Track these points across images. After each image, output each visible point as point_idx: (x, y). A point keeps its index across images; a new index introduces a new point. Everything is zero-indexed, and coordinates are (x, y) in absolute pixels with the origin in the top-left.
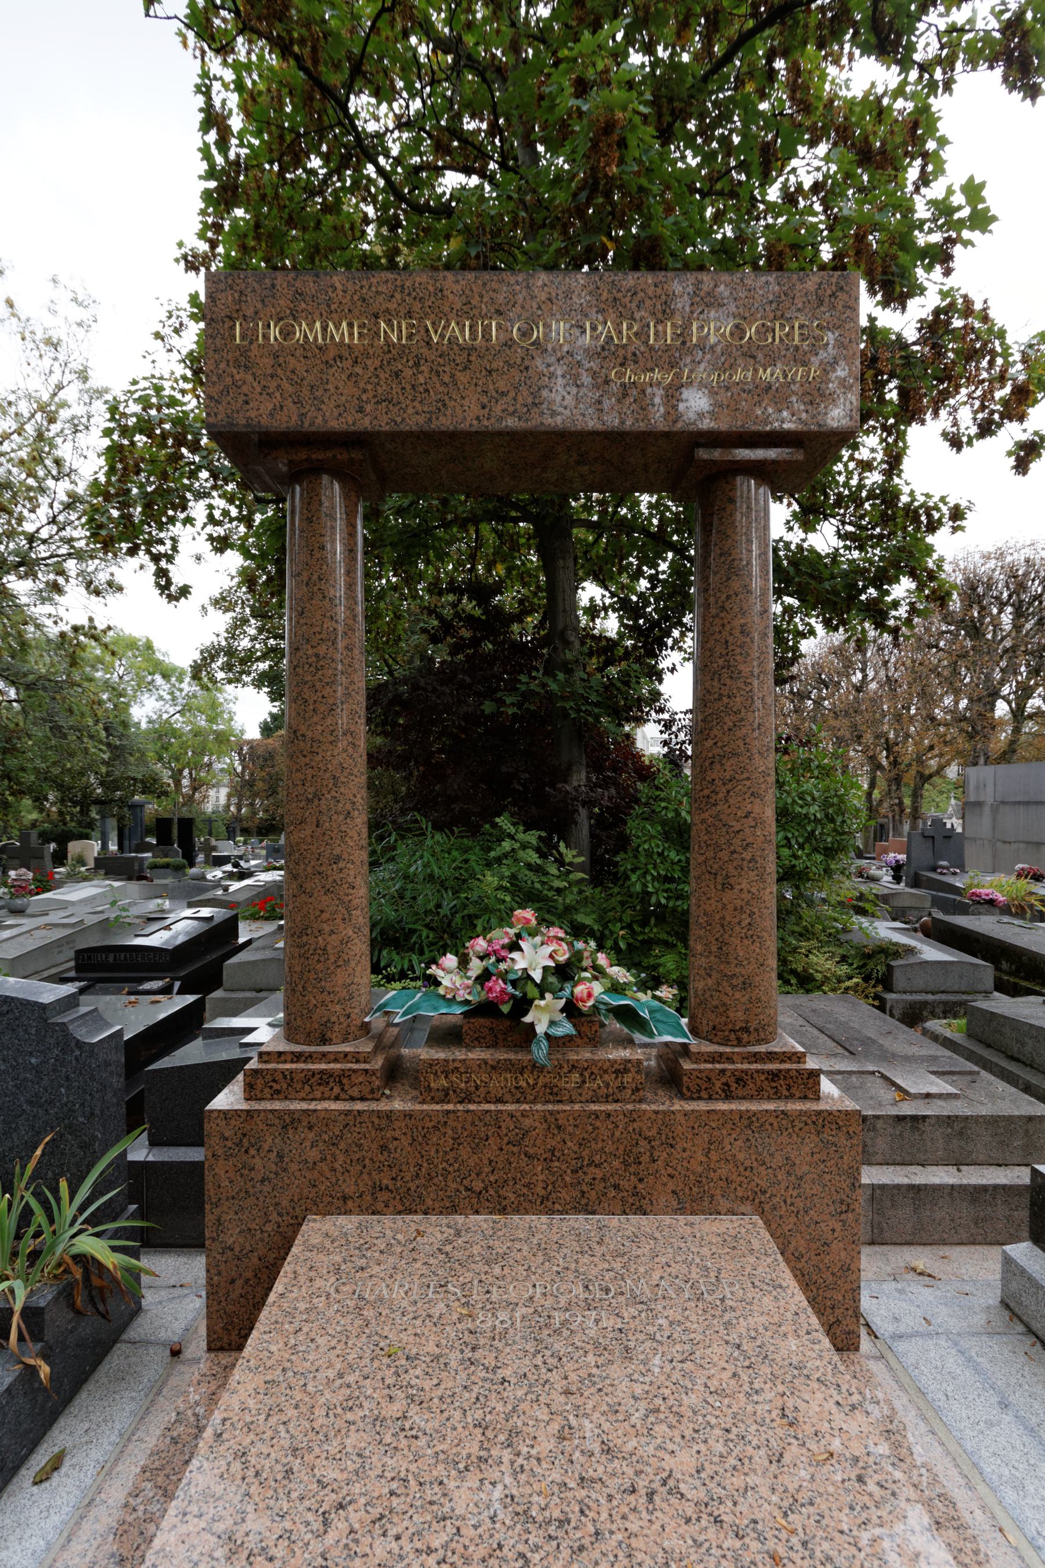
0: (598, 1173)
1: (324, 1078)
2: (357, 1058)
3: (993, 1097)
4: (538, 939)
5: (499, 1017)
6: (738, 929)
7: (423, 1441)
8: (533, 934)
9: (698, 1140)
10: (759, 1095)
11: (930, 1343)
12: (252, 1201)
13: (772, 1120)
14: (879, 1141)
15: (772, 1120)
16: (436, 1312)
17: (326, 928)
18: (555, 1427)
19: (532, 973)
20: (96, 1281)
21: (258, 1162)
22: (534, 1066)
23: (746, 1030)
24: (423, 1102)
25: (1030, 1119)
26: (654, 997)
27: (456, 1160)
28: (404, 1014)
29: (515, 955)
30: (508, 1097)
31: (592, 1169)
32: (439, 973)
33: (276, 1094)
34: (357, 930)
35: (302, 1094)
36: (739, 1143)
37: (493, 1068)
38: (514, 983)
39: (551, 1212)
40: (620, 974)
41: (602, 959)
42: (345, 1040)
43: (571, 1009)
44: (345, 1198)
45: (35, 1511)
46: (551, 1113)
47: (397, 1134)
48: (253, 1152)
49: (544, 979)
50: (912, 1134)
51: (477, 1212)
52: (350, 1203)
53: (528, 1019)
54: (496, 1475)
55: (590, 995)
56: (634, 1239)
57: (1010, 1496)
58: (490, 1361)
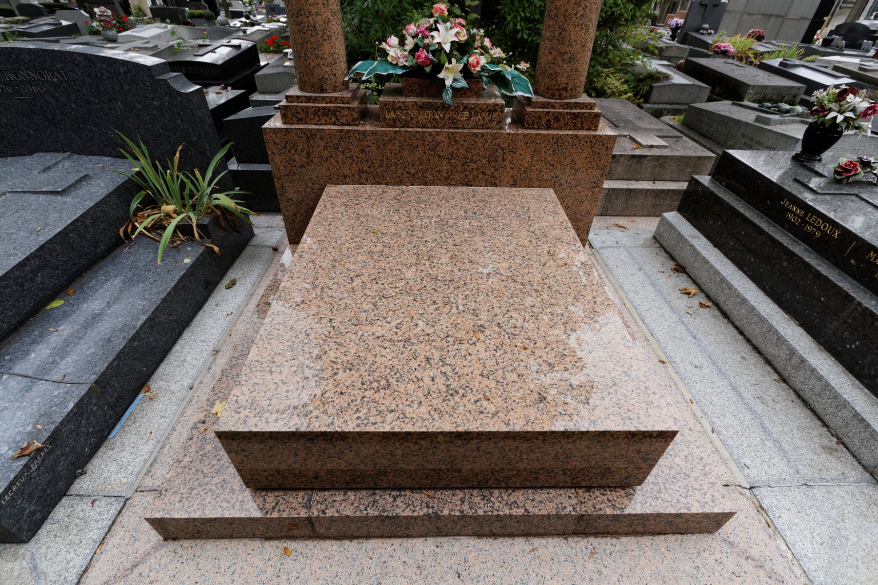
0: (475, 166)
1: (326, 112)
2: (342, 100)
3: (684, 148)
4: (448, 24)
5: (423, 76)
6: (574, 19)
7: (391, 258)
8: (445, 22)
9: (528, 150)
10: (565, 127)
11: (616, 250)
12: (297, 177)
13: (570, 140)
14: (619, 168)
15: (570, 140)
16: (394, 219)
17: (314, 11)
18: (449, 255)
19: (444, 46)
20: (229, 217)
21: (297, 157)
22: (444, 107)
23: (565, 89)
24: (382, 127)
25: (700, 158)
26: (516, 69)
27: (401, 158)
28: (368, 75)
29: (434, 33)
30: (429, 125)
31: (472, 164)
32: (387, 47)
33: (300, 121)
34: (334, 14)
35: (315, 121)
36: (550, 152)
37: (421, 107)
38: (434, 52)
39: (450, 185)
40: (497, 52)
41: (487, 42)
42: (334, 91)
43: (466, 72)
44: (345, 176)
45: (230, 297)
46: (452, 133)
47: (369, 143)
48: (293, 151)
49: (451, 51)
50: (637, 164)
51: (413, 184)
52: (348, 179)
53: (441, 76)
54: (423, 268)
55: (478, 63)
56: (490, 196)
57: (631, 295)
58: (420, 235)
